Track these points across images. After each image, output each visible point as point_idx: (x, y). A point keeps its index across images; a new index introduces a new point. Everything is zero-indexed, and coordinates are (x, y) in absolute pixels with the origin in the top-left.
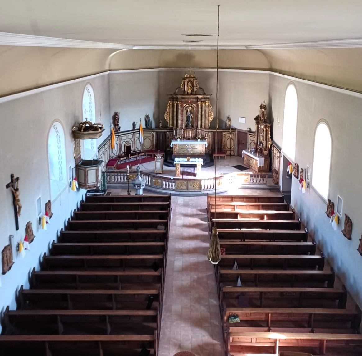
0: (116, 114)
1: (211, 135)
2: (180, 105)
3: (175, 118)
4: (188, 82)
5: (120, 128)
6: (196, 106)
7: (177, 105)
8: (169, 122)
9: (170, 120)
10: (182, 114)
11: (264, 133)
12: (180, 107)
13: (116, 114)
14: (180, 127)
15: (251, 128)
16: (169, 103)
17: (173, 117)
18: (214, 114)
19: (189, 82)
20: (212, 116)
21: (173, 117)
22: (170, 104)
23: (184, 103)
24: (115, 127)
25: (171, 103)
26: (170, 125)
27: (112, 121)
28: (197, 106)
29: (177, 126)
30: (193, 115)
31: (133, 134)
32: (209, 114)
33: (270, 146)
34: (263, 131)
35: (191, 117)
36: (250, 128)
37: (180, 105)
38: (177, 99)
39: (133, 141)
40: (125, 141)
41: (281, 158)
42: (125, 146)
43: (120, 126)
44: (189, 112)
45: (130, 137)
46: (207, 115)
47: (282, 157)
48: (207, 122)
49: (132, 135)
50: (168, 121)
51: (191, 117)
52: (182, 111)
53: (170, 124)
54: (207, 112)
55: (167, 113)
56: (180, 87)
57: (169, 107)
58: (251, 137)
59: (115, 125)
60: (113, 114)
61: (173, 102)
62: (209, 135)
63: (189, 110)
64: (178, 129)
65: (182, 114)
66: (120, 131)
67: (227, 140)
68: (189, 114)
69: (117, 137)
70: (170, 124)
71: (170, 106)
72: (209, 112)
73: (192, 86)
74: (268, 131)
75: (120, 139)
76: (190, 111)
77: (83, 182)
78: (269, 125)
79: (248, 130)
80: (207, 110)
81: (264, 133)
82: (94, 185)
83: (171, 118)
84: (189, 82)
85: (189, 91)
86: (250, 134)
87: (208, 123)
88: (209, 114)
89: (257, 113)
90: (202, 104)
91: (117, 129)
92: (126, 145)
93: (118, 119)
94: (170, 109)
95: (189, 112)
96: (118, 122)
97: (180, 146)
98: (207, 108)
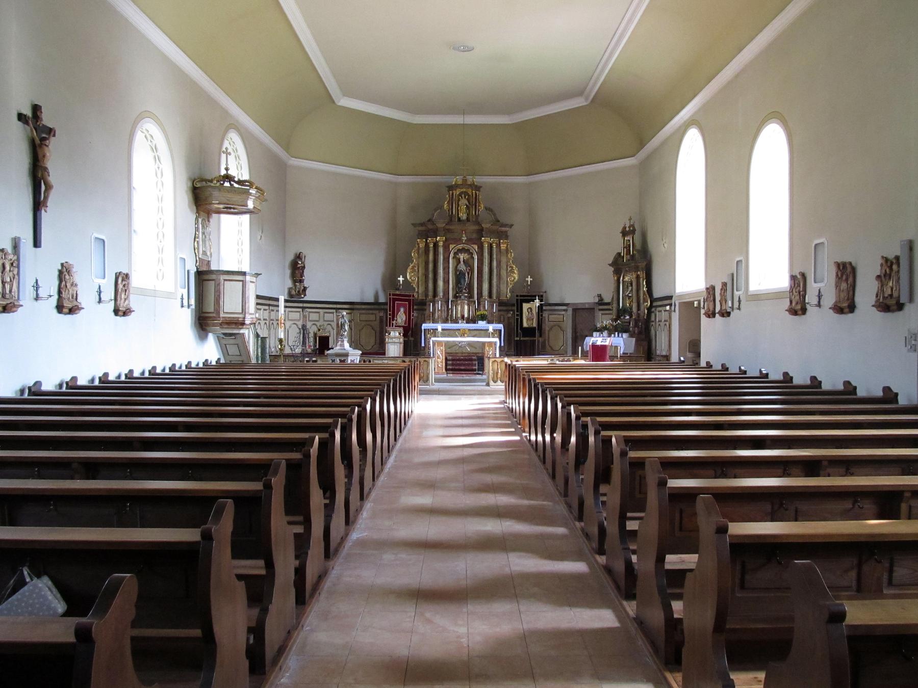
0: (298, 257)
2: (441, 244)
3: (431, 275)
4: (460, 195)
5: (305, 289)
7: (436, 245)
8: (418, 288)
9: (420, 283)
10: (446, 269)
11: (632, 290)
12: (441, 250)
13: (298, 257)
14: (441, 294)
15: (603, 296)
16: (418, 244)
17: (426, 276)
18: (519, 271)
19: (463, 196)
20: (515, 275)
21: (426, 276)
22: (419, 247)
24: (295, 286)
25: (422, 245)
27: (288, 272)
28: (481, 247)
29: (435, 294)
30: (472, 270)
31: (334, 311)
33: (646, 311)
34: (629, 285)
36: (599, 296)
37: (441, 244)
38: (435, 233)
39: (335, 328)
40: (317, 326)
41: (673, 313)
42: (315, 335)
43: (306, 284)
44: (462, 263)
45: (328, 317)
46: (504, 273)
47: (675, 311)
48: (503, 287)
49: (333, 313)
50: (414, 286)
52: (446, 260)
54: (504, 265)
55: (413, 267)
56: (441, 207)
57: (418, 254)
58: (602, 314)
59: (295, 282)
60: (291, 257)
61: (426, 240)
63: (462, 260)
64: (436, 298)
65: (446, 269)
66: (306, 299)
67: (549, 331)
68: (462, 267)
69: (300, 312)
70: (420, 292)
71: (420, 252)
72: (507, 266)
73: (467, 203)
74: (641, 279)
75: (304, 317)
76: (464, 261)
77: (211, 309)
78: (643, 265)
79: (597, 300)
80: (504, 260)
81: (632, 290)
82: (239, 318)
83: (422, 278)
84: (463, 196)
85: (463, 216)
86: (600, 310)
87: (505, 290)
88: (507, 269)
89: (617, 245)
90: (491, 244)
91: (299, 291)
92: (319, 334)
93: (304, 267)
94: (419, 258)
96: (302, 275)
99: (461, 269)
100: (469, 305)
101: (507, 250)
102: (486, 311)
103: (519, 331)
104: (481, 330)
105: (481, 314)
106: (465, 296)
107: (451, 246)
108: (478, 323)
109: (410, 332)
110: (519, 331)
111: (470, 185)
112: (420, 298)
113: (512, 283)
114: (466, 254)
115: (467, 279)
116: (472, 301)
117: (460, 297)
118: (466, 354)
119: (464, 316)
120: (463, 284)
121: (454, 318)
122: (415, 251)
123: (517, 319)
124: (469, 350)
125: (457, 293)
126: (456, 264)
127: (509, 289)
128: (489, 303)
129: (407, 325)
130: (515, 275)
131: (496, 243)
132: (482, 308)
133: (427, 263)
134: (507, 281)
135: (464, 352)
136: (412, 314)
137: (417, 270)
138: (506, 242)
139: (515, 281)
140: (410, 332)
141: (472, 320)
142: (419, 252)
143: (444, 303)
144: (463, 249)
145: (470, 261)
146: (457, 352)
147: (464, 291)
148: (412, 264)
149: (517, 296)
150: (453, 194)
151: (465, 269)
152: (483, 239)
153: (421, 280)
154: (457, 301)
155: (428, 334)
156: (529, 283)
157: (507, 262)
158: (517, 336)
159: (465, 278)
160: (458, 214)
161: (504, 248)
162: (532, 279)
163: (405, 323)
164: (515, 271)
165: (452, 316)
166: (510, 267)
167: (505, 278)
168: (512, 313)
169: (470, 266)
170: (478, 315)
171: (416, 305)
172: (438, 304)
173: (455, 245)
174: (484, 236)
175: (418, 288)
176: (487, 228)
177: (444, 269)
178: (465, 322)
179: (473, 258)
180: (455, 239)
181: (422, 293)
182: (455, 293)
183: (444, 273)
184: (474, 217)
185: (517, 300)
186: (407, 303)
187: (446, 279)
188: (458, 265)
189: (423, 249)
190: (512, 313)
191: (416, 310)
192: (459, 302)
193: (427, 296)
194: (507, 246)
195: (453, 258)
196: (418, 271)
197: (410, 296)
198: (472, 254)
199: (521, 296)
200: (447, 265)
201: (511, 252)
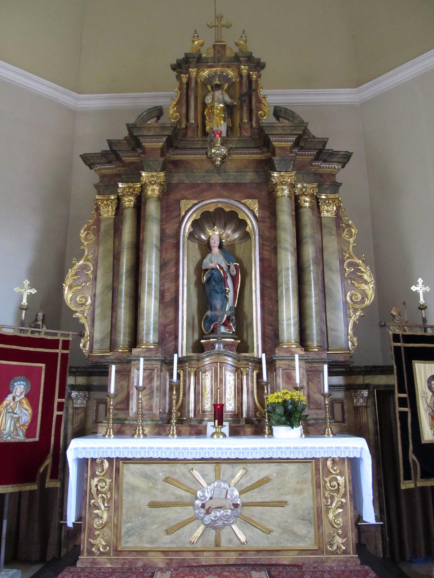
1: (370, 411)
6: (261, 207)
8: (92, 325)
9: (97, 311)
20: (364, 287)
23: (186, 193)
26: (96, 347)
32: (343, 270)
35: (229, 282)
44: (216, 250)
51: (229, 282)
53: (97, 336)
57: (97, 232)
62: (357, 409)
63: (215, 243)
70: (97, 336)
72: (342, 262)
76: (221, 246)
88: (343, 270)
95: (216, 250)
97: (146, 477)
98: (330, 234)
99: (212, 265)
100: (238, 371)
101: (338, 218)
102: (296, 389)
103: (412, 457)
104: (288, 461)
105: (285, 402)
106: (226, 345)
107: (184, 204)
108: (271, 433)
109: (48, 461)
110: (412, 457)
111: (237, 59)
112: (96, 353)
113: (358, 306)
114: (229, 232)
115: (230, 296)
116: (248, 360)
117: (212, 346)
118: (232, 558)
119: (222, 406)
120: (218, 307)
121: (192, 415)
122: (88, 229)
123: (403, 415)
124: (243, 539)
125: (202, 335)
126: (199, 257)
127: (350, 327)
128: (303, 363)
129: (37, 439)
130: (364, 287)
131: (312, 196)
132: (280, 381)
133: (117, 258)
134: (345, 303)
135: (224, 545)
136: (57, 400)
137: (91, 276)
138: (334, 200)
139: (367, 302)
140: (48, 461)
141: (248, 421)
142: (98, 229)
143: (158, 365)
144: (219, 211)
145: (239, 251)
146: (199, 546)
147: (223, 329)
148: (78, 261)
149: (396, 338)
150: (189, 79)
151: (224, 265)
152: (275, 174)
153: (102, 304)
154: (199, 360)
155: (94, 475)
156: (422, 300)
157: (341, 252)
158: (407, 477)
159: (225, 293)
160: (204, 126)
161: (329, 215)
162: (428, 289)
163: (30, 432)
164: (366, 277)
165: (183, 408)
166: (351, 264)
167: (340, 297)
168: (365, 393)
169: (238, 260)
170: (274, 406)
171: (74, 374)
172: (138, 369)
173: (196, 202)
174: (278, 170)
175: (92, 325)
176: (282, 148)
177: (163, 266)
178: (226, 429)
179: (246, 236)
180: (194, 186)
181: (102, 340)
182: (196, 337)
183: (162, 278)
184: (247, 126)
185: (397, 350)
186: (43, 365)
187: (168, 297)
188: (203, 257)
189: (112, 221)
190: (365, 393)
191: (74, 387)
192: (207, 361)
193: (113, 346)
194: (338, 208)
195: (191, 235)
196: (95, 278)
197: (54, 344)
198: (242, 224)
199: (408, 339)
200: (170, 255)
201: (348, 226)
